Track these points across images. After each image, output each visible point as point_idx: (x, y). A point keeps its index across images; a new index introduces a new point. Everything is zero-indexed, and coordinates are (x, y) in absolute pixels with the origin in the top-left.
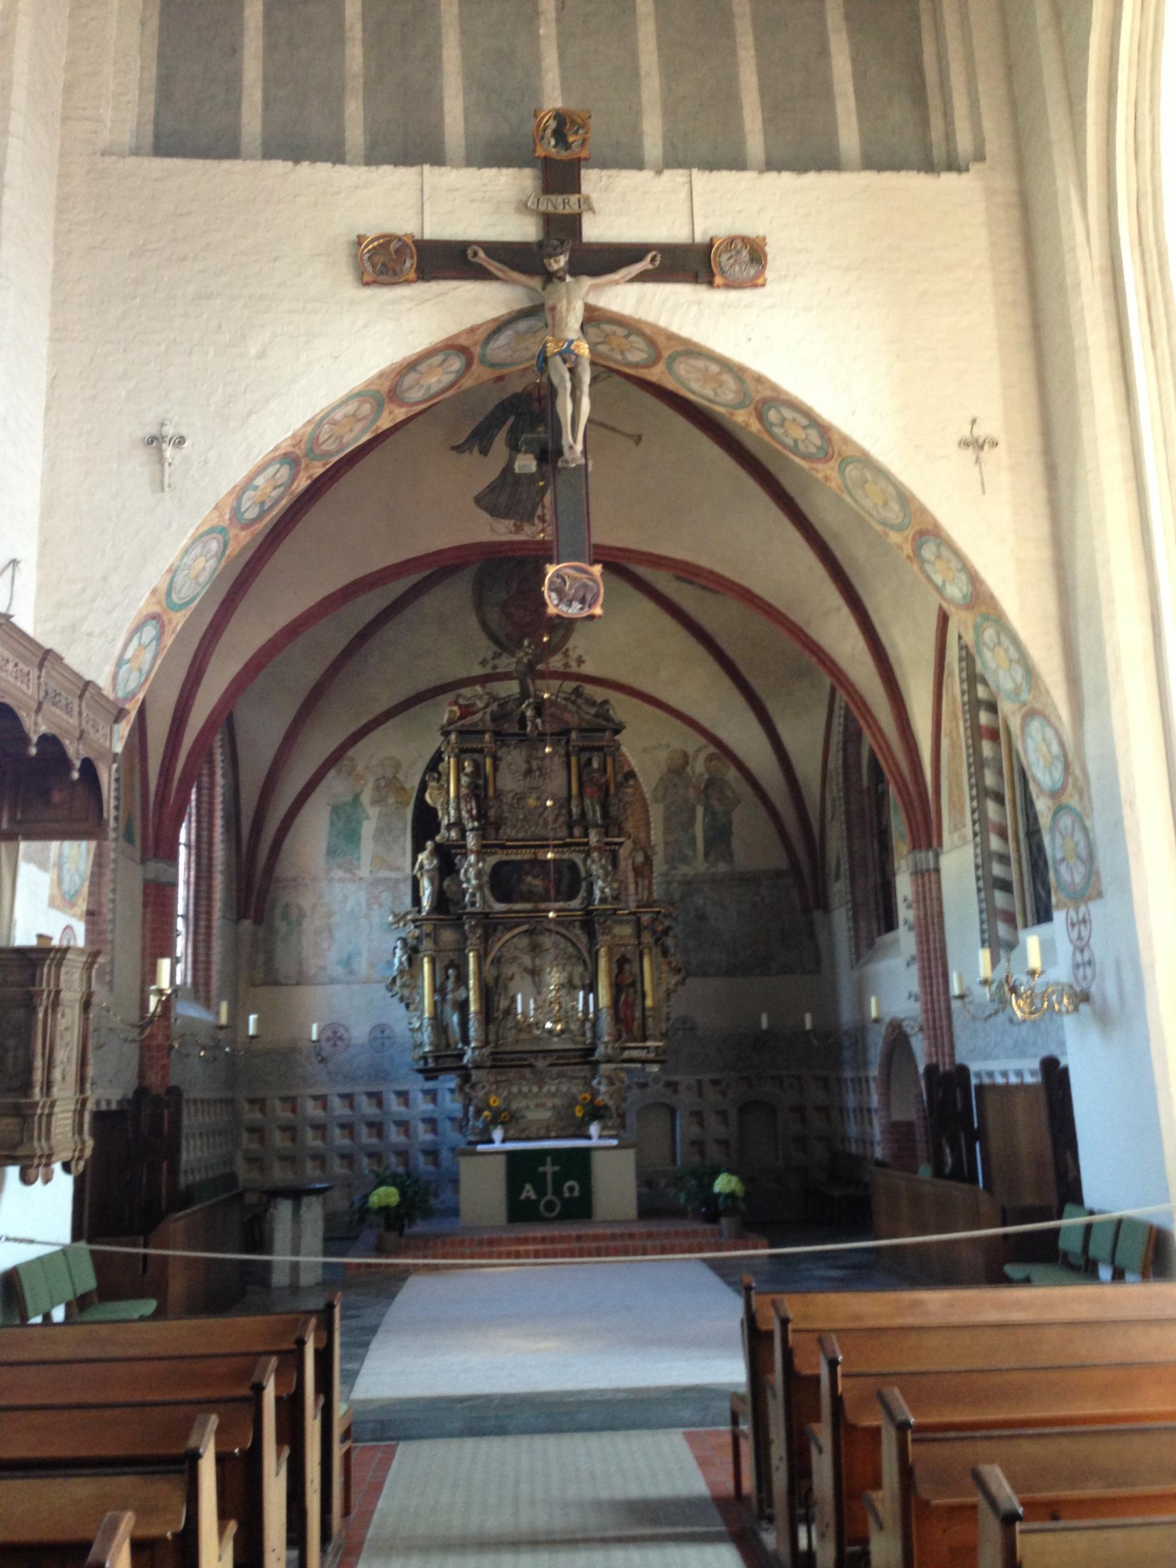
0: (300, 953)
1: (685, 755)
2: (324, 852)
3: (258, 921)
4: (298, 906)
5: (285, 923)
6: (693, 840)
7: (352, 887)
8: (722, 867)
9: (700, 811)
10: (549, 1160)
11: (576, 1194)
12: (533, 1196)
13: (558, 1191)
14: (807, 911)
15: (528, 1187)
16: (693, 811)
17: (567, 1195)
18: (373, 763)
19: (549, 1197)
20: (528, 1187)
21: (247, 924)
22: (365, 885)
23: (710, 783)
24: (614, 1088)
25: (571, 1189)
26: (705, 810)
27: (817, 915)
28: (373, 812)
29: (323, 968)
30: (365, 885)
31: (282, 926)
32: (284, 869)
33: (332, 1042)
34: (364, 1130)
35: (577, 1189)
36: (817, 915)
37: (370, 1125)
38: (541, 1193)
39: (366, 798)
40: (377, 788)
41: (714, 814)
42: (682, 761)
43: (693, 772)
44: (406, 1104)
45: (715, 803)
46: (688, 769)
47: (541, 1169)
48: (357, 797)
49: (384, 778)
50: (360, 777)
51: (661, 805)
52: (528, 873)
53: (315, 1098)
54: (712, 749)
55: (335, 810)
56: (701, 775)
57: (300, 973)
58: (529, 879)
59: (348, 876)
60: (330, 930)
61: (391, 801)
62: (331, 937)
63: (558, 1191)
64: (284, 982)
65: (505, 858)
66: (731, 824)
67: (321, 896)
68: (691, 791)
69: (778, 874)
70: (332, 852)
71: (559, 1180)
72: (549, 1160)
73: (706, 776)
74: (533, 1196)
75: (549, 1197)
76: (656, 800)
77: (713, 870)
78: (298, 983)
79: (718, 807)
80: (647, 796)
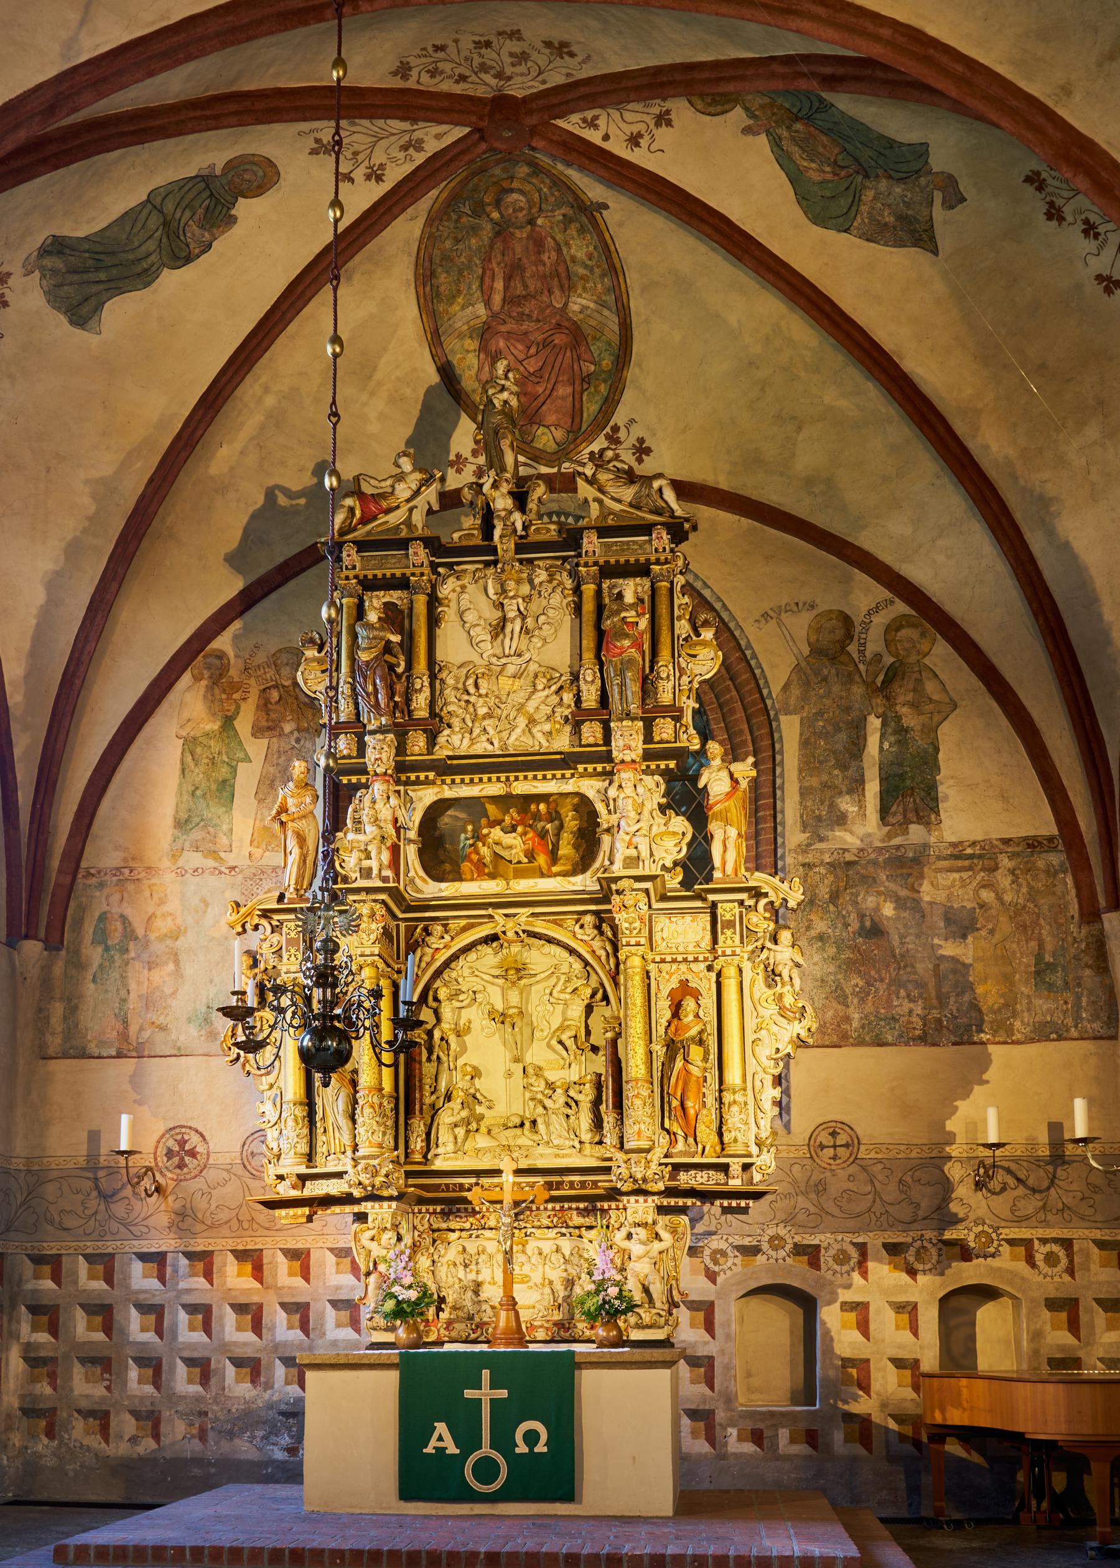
0: (124, 1001)
2: (169, 821)
3: (54, 943)
4: (124, 919)
5: (100, 949)
7: (213, 881)
10: (486, 1374)
11: (541, 1448)
12: (452, 1449)
13: (503, 1441)
15: (441, 1428)
17: (522, 1448)
18: (261, 658)
19: (486, 1450)
20: (441, 1428)
21: (32, 948)
22: (240, 877)
24: (657, 1246)
25: (531, 1437)
28: (256, 748)
29: (163, 1028)
30: (240, 877)
31: (94, 955)
32: (103, 854)
33: (176, 1160)
34: (230, 1317)
35: (544, 1437)
37: (240, 1309)
38: (468, 1440)
39: (244, 724)
40: (264, 705)
41: (902, 731)
44: (306, 1275)
47: (469, 1393)
48: (228, 722)
49: (276, 687)
50: (234, 687)
52: (492, 824)
53: (144, 1257)
55: (190, 744)
57: (124, 1036)
58: (496, 833)
59: (211, 863)
60: (177, 962)
61: (288, 727)
62: (178, 973)
63: (503, 1441)
64: (96, 1052)
65: (448, 793)
67: (162, 902)
69: (1033, 844)
70: (182, 824)
71: (504, 1418)
72: (486, 1374)
74: (452, 1449)
75: (486, 1450)
78: (119, 1055)
79: (910, 719)
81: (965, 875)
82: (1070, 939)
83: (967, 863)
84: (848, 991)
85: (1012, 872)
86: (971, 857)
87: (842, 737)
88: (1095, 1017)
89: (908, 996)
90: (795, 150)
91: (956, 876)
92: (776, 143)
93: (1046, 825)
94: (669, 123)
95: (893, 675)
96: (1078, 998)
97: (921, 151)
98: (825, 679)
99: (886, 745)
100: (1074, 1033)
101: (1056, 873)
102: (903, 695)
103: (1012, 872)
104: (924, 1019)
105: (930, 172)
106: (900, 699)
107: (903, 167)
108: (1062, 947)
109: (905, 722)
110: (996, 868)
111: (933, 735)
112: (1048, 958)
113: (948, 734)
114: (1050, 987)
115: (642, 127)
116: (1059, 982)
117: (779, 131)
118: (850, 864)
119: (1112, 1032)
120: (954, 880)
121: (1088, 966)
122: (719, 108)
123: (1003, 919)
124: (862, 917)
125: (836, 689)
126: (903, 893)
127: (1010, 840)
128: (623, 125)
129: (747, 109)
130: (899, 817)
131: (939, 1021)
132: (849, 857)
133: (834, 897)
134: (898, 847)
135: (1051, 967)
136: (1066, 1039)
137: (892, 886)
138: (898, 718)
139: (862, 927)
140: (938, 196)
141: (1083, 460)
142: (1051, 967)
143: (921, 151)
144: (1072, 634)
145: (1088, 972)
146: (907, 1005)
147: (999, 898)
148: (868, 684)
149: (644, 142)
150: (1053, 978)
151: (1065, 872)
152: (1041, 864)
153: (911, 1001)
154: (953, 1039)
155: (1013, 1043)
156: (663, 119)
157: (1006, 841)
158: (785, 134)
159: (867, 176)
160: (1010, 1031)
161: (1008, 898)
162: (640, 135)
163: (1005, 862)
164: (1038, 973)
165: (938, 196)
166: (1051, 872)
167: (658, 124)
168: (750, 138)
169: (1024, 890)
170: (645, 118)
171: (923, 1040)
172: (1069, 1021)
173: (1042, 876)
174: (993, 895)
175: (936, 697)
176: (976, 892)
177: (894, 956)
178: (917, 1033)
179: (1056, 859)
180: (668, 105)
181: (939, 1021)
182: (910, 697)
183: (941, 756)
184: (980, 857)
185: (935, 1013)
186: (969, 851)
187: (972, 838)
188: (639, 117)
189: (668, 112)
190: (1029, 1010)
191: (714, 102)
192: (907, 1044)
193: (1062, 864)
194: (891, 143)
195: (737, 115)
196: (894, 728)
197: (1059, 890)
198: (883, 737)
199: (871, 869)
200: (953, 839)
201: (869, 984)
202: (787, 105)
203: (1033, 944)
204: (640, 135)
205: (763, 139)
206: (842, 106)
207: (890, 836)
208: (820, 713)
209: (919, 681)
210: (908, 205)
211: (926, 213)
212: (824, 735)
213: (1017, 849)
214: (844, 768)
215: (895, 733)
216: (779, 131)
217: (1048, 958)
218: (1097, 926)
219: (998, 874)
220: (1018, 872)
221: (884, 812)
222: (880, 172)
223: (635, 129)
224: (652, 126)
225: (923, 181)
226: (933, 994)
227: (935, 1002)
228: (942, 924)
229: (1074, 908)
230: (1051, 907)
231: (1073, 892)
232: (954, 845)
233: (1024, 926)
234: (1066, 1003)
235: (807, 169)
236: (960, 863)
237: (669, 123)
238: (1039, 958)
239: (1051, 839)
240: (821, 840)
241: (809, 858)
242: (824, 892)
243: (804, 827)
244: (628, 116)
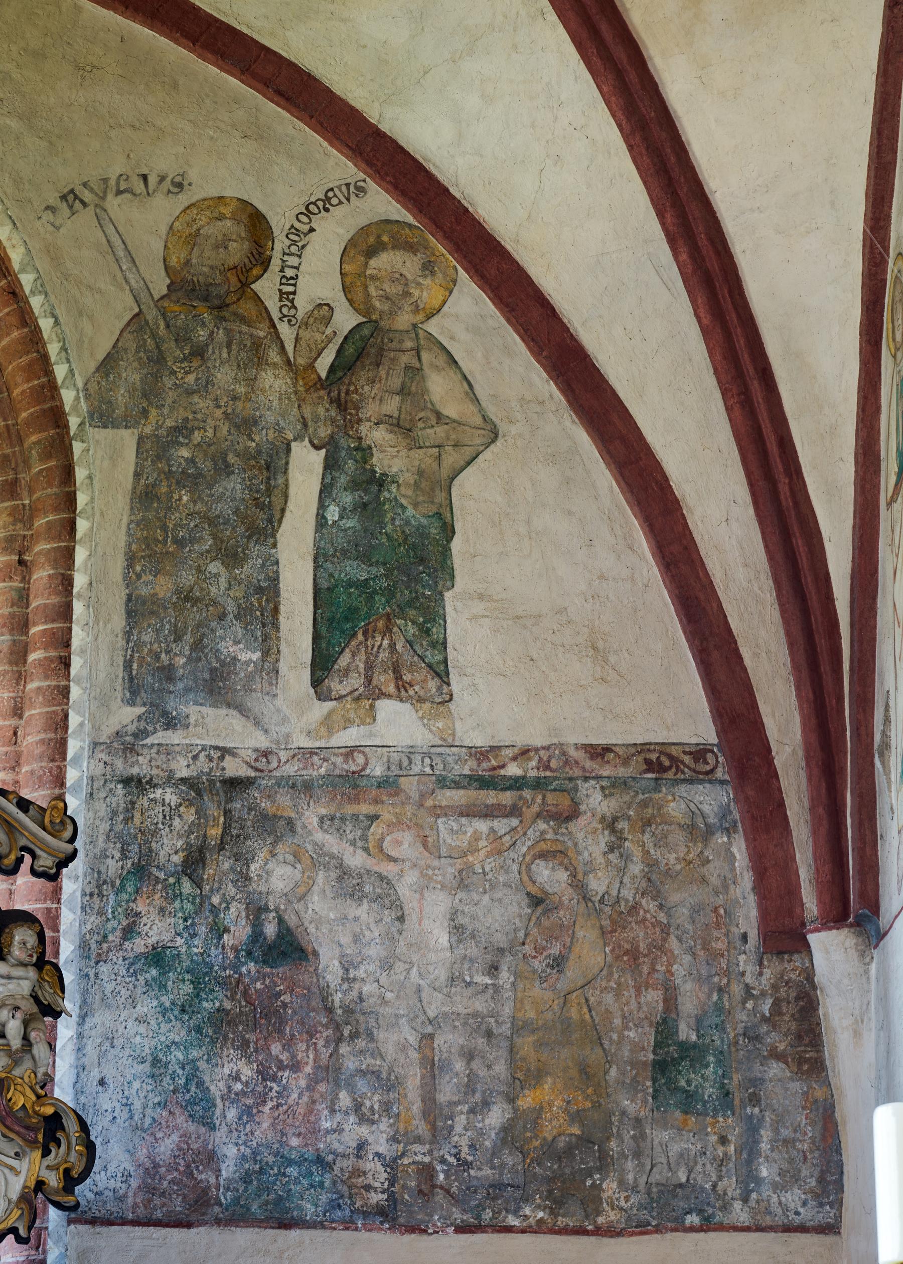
1: (256, 224)
6: (268, 592)
8: (397, 725)
9: (305, 468)
14: (784, 936)
16: (272, 465)
23: (363, 350)
26: (330, 465)
27: (830, 950)
36: (830, 950)
41: (372, 482)
42: (237, 252)
43: (287, 298)
45: (377, 436)
46: (266, 287)
51: (128, 439)
54: (381, 204)
56: (323, 312)
66: (449, 531)
68: (274, 383)
69: (662, 763)
73: (346, 320)
76: (103, 416)
79: (391, 457)
80: (68, 396)
81: (502, 825)
82: (737, 989)
83: (507, 798)
84: (216, 1089)
85: (610, 824)
86: (517, 784)
87: (234, 486)
88: (789, 1178)
89: (358, 1107)
91: (482, 826)
93: (690, 720)
96: (752, 1129)
99: (333, 513)
100: (740, 1214)
101: (710, 831)
102: (378, 401)
103: (610, 824)
104: (391, 1165)
106: (370, 410)
108: (719, 1009)
109: (380, 462)
110: (574, 814)
111: (440, 497)
112: (686, 1033)
113: (475, 495)
114: (689, 1101)
116: (710, 1091)
118: (235, 785)
119: (826, 1215)
120: (476, 837)
121: (779, 1057)
123: (587, 934)
124: (257, 911)
125: (224, 376)
126: (356, 860)
127: (607, 749)
130: (356, 682)
131: (426, 1172)
132: (234, 768)
133: (194, 862)
134: (350, 752)
135: (692, 1054)
136: (721, 1228)
137: (331, 842)
138: (364, 452)
139: (257, 935)
142: (692, 1054)
145: (775, 1069)
146: (354, 1131)
147: (578, 885)
150: (696, 1079)
151: (729, 831)
152: (675, 809)
153: (364, 1119)
154: (458, 1216)
155: (598, 1232)
157: (599, 752)
160: (592, 1202)
161: (597, 884)
163: (595, 801)
164: (662, 1067)
166: (698, 831)
169: (636, 868)
171: (389, 1215)
172: (730, 1185)
173: (678, 837)
174: (563, 876)
175: (450, 411)
176: (526, 868)
177: (330, 1010)
178: (376, 1198)
179: (711, 799)
181: (426, 1172)
182: (392, 406)
183: (456, 545)
184: (538, 785)
185: (419, 1153)
186: (513, 770)
187: (522, 739)
190: (637, 1154)
192: (348, 1225)
193: (724, 813)
196: (354, 476)
197: (714, 871)
198: (326, 491)
199: (284, 800)
200: (479, 740)
201: (264, 1074)
203: (653, 997)
207: (328, 724)
208: (183, 430)
212: (191, 479)
213: (622, 772)
214: (232, 557)
215: (354, 485)
217: (686, 1033)
218: (798, 961)
219: (578, 827)
220: (622, 825)
221: (322, 666)
226: (416, 1108)
227: (421, 1128)
228: (444, 939)
229: (748, 917)
230: (697, 910)
231: (747, 880)
232: (480, 754)
233: (634, 954)
234: (723, 1140)
236: (491, 797)
238: (665, 1029)
239: (700, 753)
240: (171, 723)
241: (141, 767)
242: (170, 848)
243: (134, 689)
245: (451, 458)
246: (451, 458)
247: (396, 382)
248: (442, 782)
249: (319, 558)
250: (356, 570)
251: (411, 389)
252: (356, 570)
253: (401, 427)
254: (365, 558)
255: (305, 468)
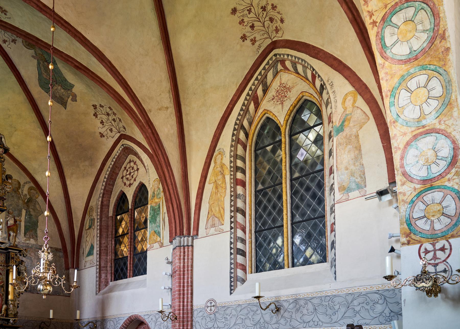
9: (24, 212)
16: (20, 211)
26: (26, 212)
41: (30, 215)
45: (31, 210)
68: (21, 202)
77: (28, 242)
79: (32, 213)
90: (42, 68)
92: (39, 64)
93: (60, 246)
94: (15, 43)
95: (30, 200)
97: (72, 86)
98: (13, 196)
99: (26, 218)
102: (31, 207)
105: (71, 91)
106: (30, 207)
107: (66, 87)
115: (8, 40)
117: (41, 62)
122: (29, 47)
125: (16, 200)
128: (4, 36)
129: (35, 52)
138: (30, 212)
140: (71, 97)
141: (83, 168)
143: (72, 86)
144: (72, 205)
148: (24, 201)
149: (7, 43)
152: (58, 254)
156: (14, 41)
158: (42, 63)
159: (57, 84)
162: (7, 41)
165: (71, 97)
167: (12, 41)
168: (33, 59)
170: (10, 38)
179: (61, 254)
180: (17, 39)
182: (33, 207)
188: (8, 37)
189: (16, 40)
191: (28, 45)
194: (66, 80)
195: (32, 52)
198: (26, 215)
200: (40, 244)
202: (46, 57)
204: (7, 41)
205: (36, 61)
206: (59, 66)
209: (35, 204)
210: (63, 95)
211: (67, 99)
215: (29, 215)
216: (41, 62)
222: (60, 84)
223: (6, 39)
224: (11, 41)
225: (69, 92)
235: (43, 74)
237: (15, 43)
239: (60, 249)
244: (6, 34)
245: (38, 214)
246: (38, 214)
247: (33, 205)
248: (36, 248)
249: (25, 222)
250: (28, 224)
251: (35, 206)
252: (28, 224)
253: (34, 210)
254: (30, 223)
255: (24, 212)
